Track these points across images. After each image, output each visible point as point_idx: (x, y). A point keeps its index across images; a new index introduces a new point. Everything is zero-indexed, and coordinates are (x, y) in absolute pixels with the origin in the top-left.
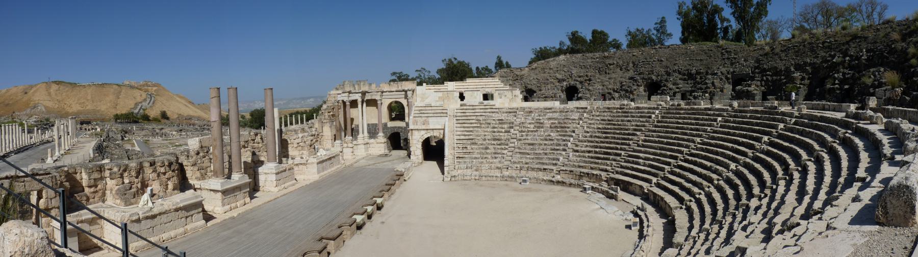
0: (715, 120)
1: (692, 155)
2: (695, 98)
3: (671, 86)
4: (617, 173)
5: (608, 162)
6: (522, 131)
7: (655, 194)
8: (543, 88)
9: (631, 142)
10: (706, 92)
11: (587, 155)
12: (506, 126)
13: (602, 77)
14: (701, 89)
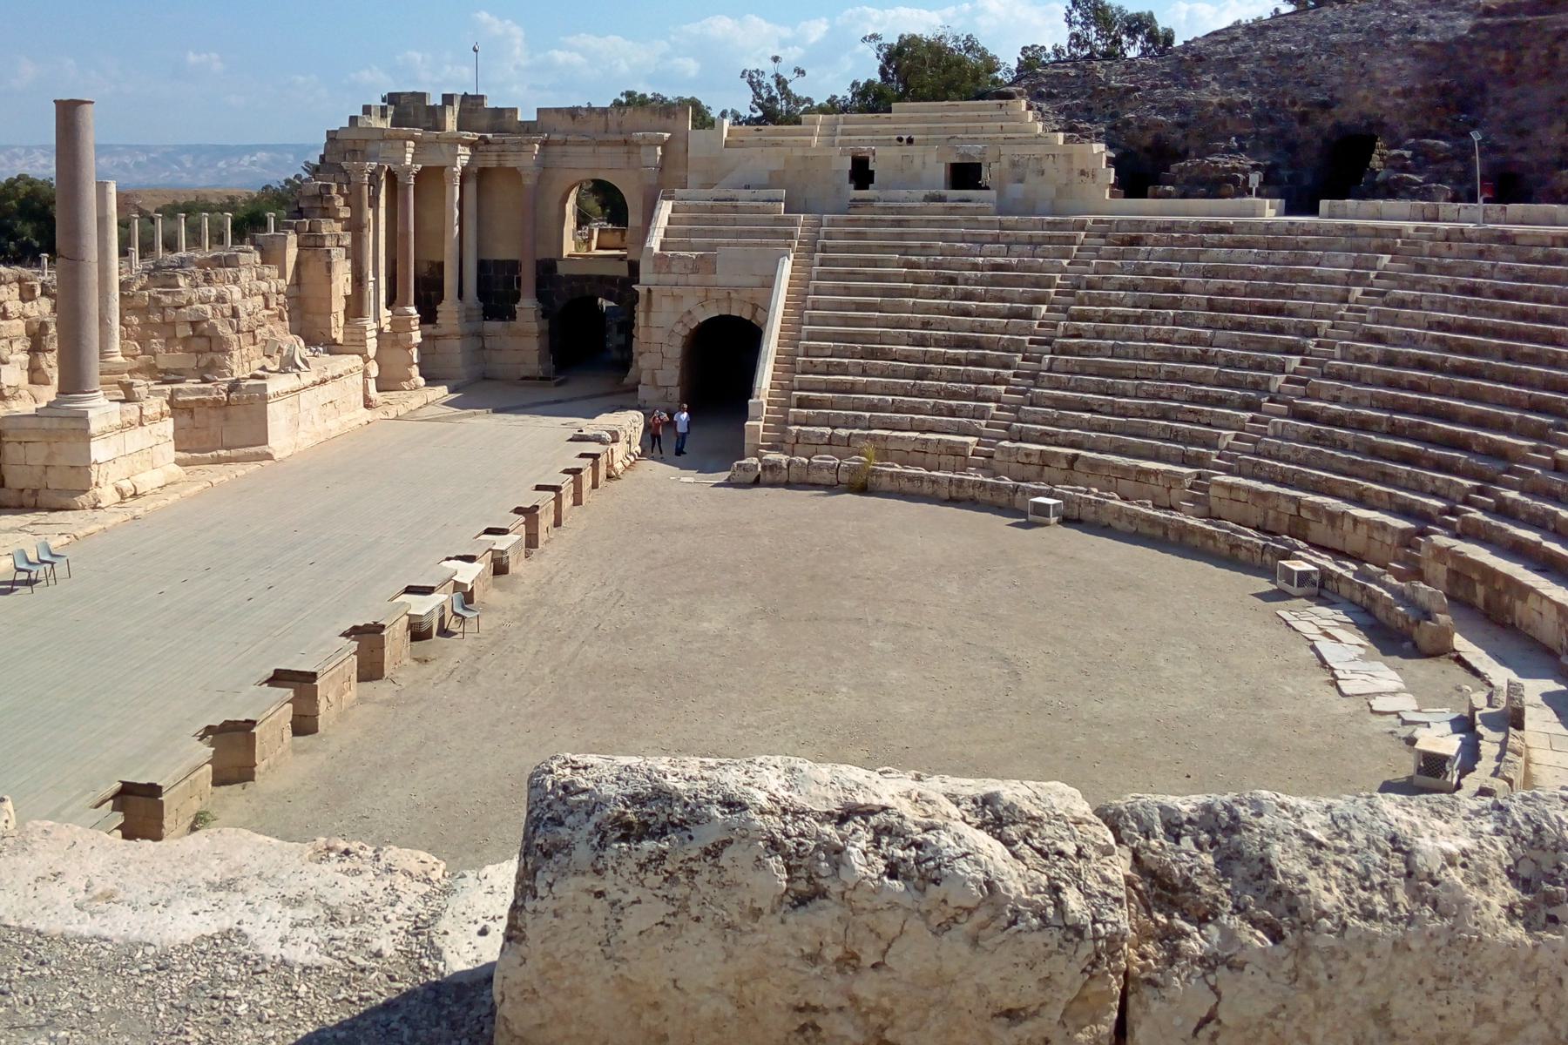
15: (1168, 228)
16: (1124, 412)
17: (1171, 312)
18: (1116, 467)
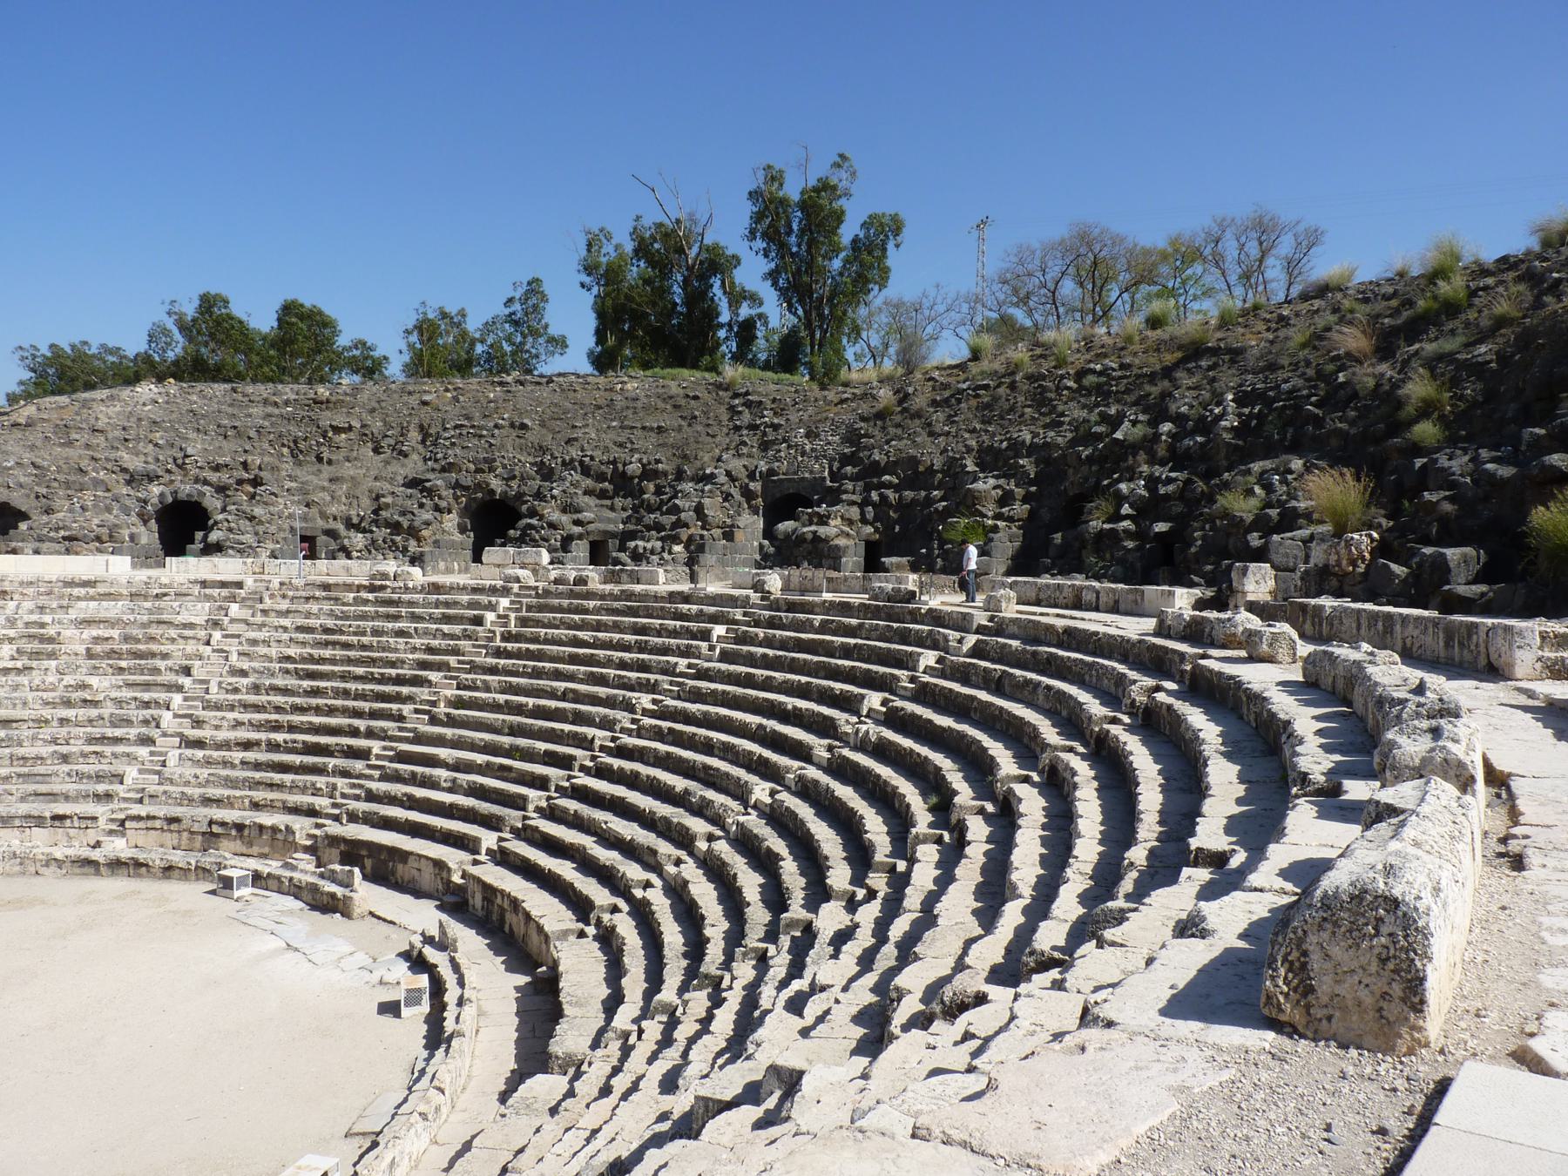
0: (705, 635)
1: (623, 752)
2: (637, 557)
3: (556, 516)
4: (353, 817)
5: (321, 781)
7: (489, 891)
8: (60, 503)
9: (407, 709)
10: (676, 539)
11: (237, 756)
13: (304, 474)
14: (658, 527)
17: (53, 663)
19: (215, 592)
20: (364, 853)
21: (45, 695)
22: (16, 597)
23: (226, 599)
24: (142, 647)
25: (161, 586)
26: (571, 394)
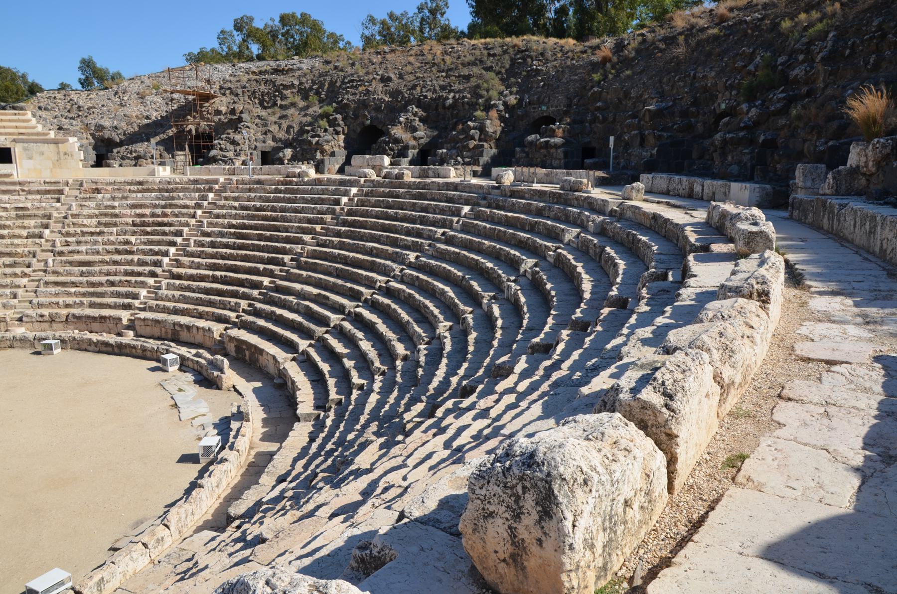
0: (457, 213)
6: (68, 234)
9: (287, 258)
12: (32, 223)
15: (111, 184)
16: (93, 285)
17: (115, 229)
18: (88, 317)
19: (202, 186)
20: (244, 347)
21: (107, 247)
22: (103, 191)
23: (205, 190)
24: (160, 219)
25: (178, 183)
26: (421, 58)
